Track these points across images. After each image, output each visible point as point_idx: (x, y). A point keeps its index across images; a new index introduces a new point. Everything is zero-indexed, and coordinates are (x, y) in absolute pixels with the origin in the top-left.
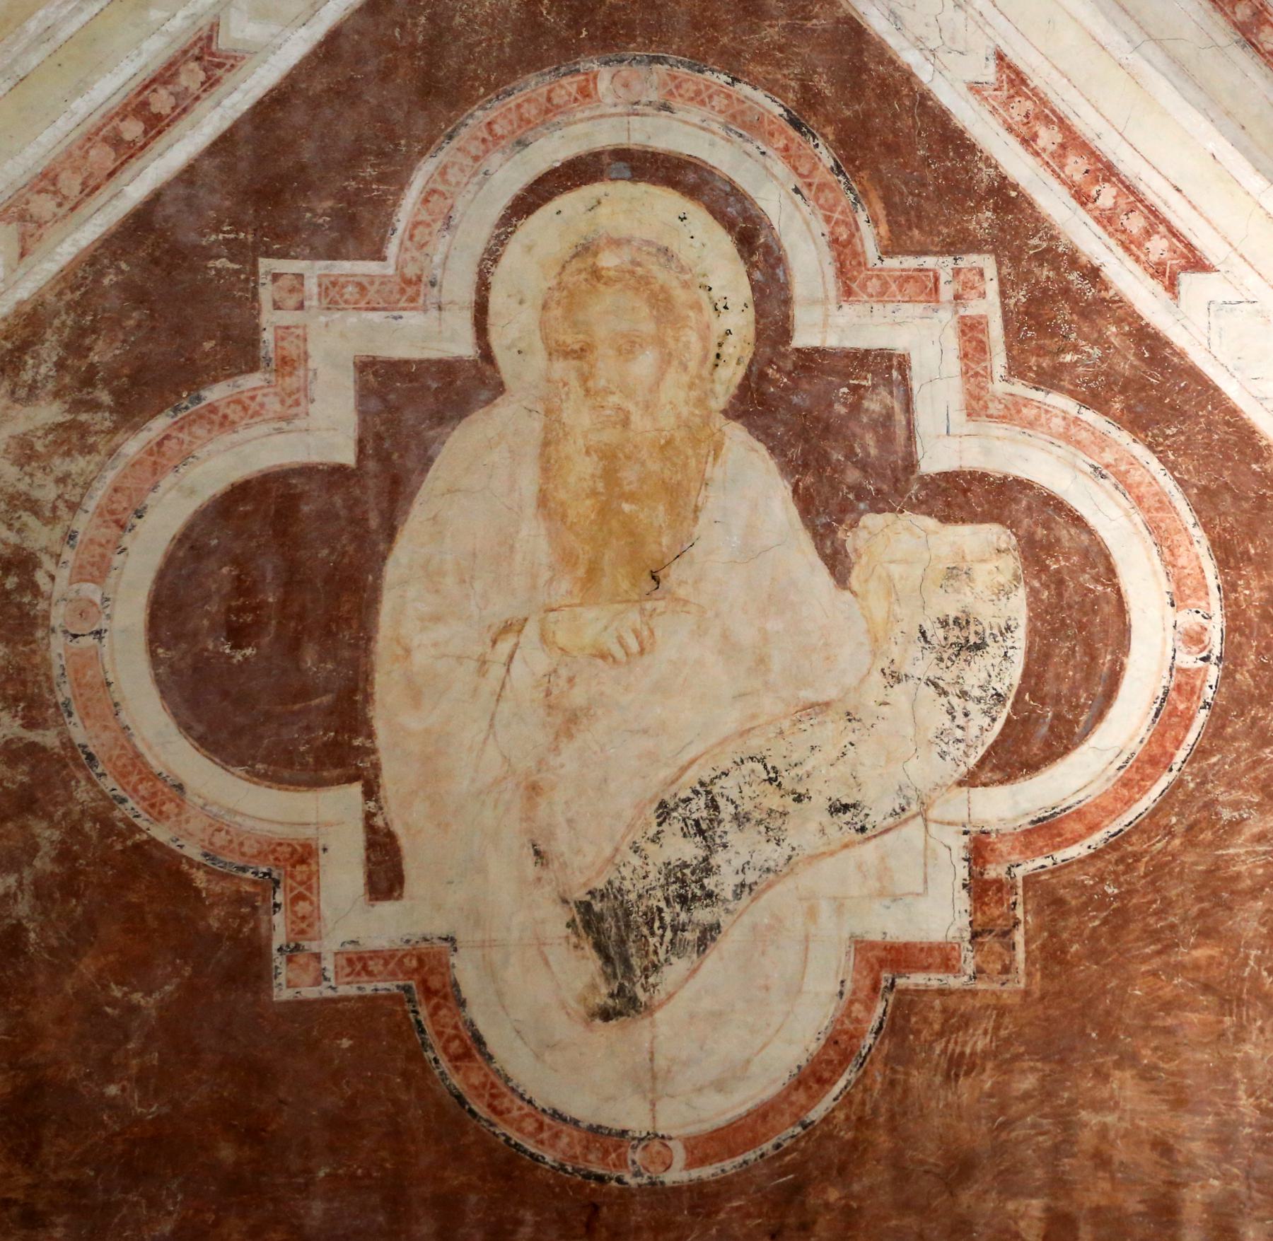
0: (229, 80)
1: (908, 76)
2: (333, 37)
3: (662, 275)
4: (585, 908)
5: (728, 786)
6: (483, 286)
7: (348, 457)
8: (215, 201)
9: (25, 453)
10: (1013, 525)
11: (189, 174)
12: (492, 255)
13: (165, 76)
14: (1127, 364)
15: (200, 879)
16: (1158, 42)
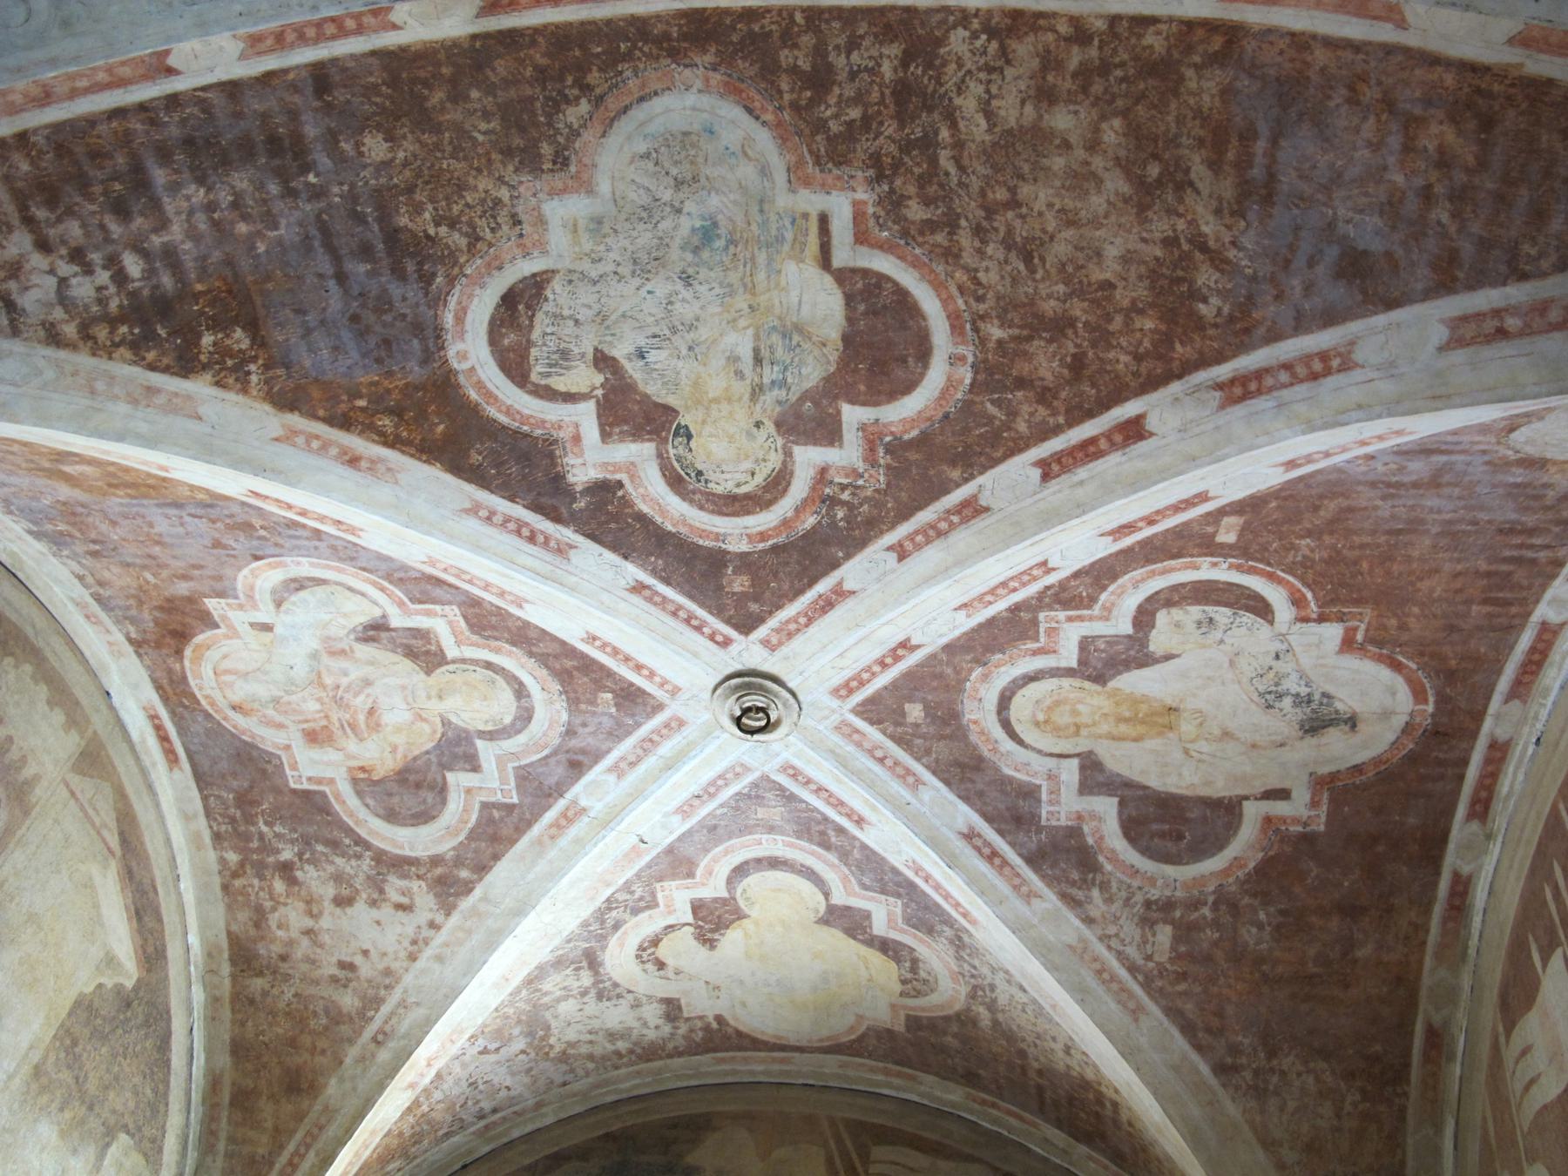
0: (977, 829)
1: (965, 634)
2: (960, 797)
3: (1048, 702)
4: (1306, 732)
5: (1262, 688)
6: (1051, 755)
7: (1115, 800)
8: (1021, 837)
9: (1109, 900)
10: (1157, 610)
11: (1012, 845)
12: (1039, 752)
13: (978, 849)
14: (1088, 580)
15: (1271, 853)
16: (947, 569)
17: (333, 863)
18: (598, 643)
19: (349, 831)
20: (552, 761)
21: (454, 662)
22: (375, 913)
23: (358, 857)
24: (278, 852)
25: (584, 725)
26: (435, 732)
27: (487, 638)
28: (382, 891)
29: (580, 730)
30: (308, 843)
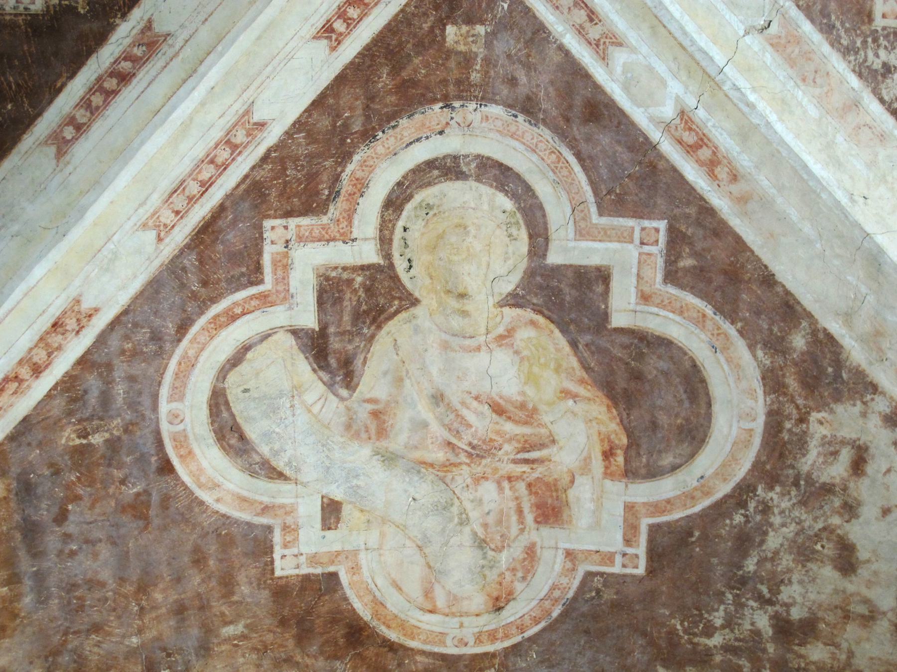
17: (776, 553)
18: (339, 26)
19: (719, 510)
20: (583, 147)
21: (388, 256)
22: (869, 511)
23: (766, 509)
24: (756, 633)
25: (513, 82)
26: (533, 323)
27: (334, 194)
28: (828, 489)
29: (523, 90)
30: (743, 581)
